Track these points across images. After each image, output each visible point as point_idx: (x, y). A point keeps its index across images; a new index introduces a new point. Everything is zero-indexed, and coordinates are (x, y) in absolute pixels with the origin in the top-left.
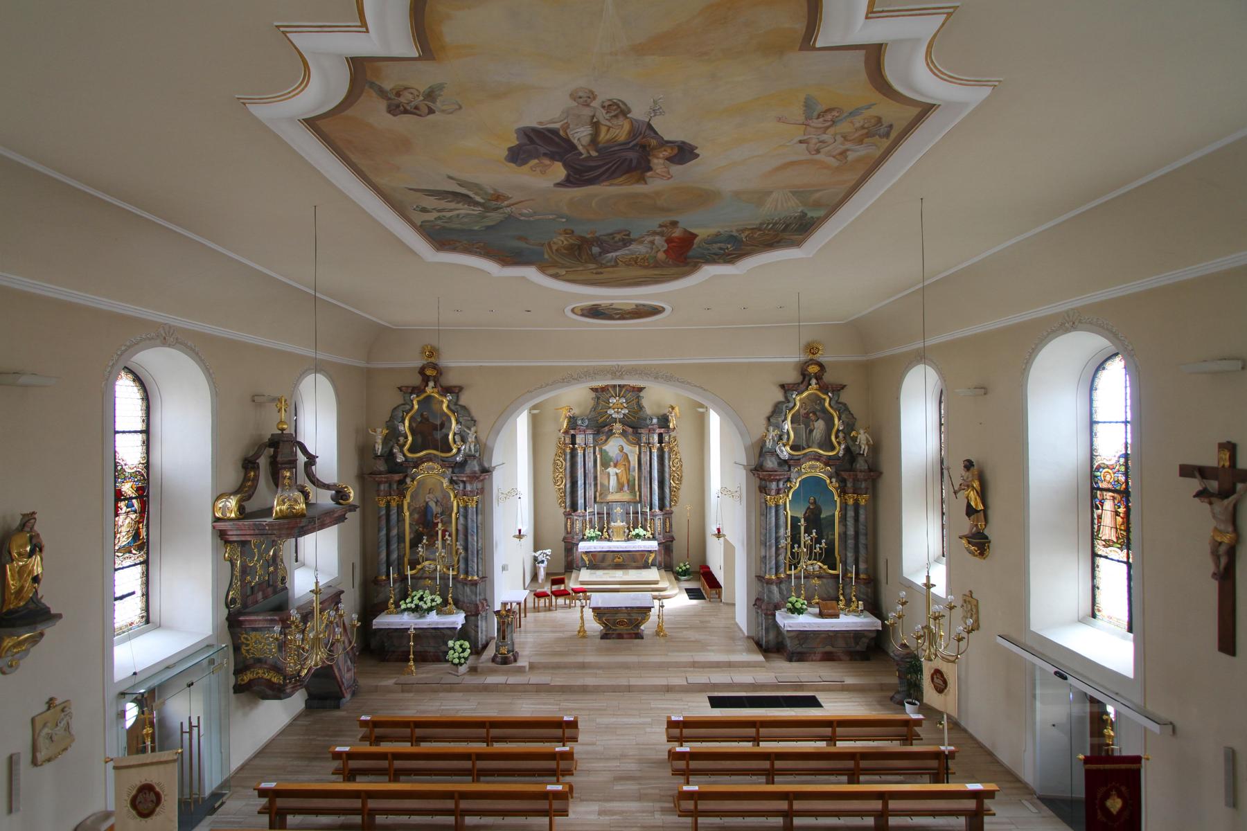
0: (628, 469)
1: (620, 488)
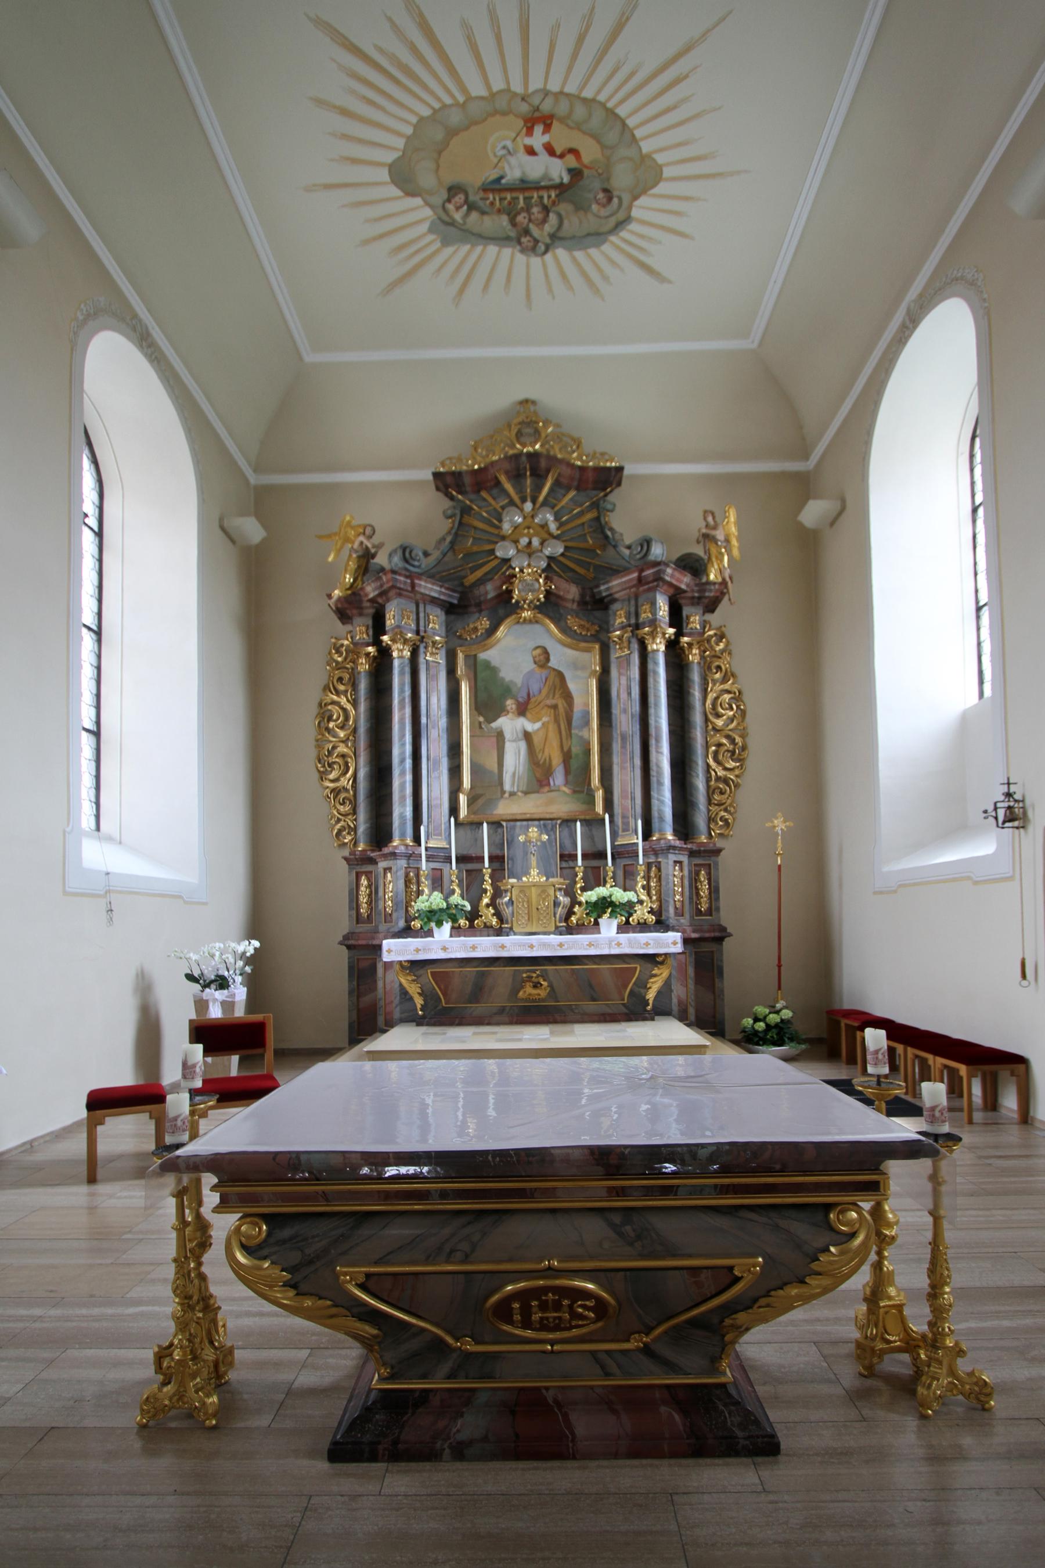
0: (565, 716)
1: (539, 777)
